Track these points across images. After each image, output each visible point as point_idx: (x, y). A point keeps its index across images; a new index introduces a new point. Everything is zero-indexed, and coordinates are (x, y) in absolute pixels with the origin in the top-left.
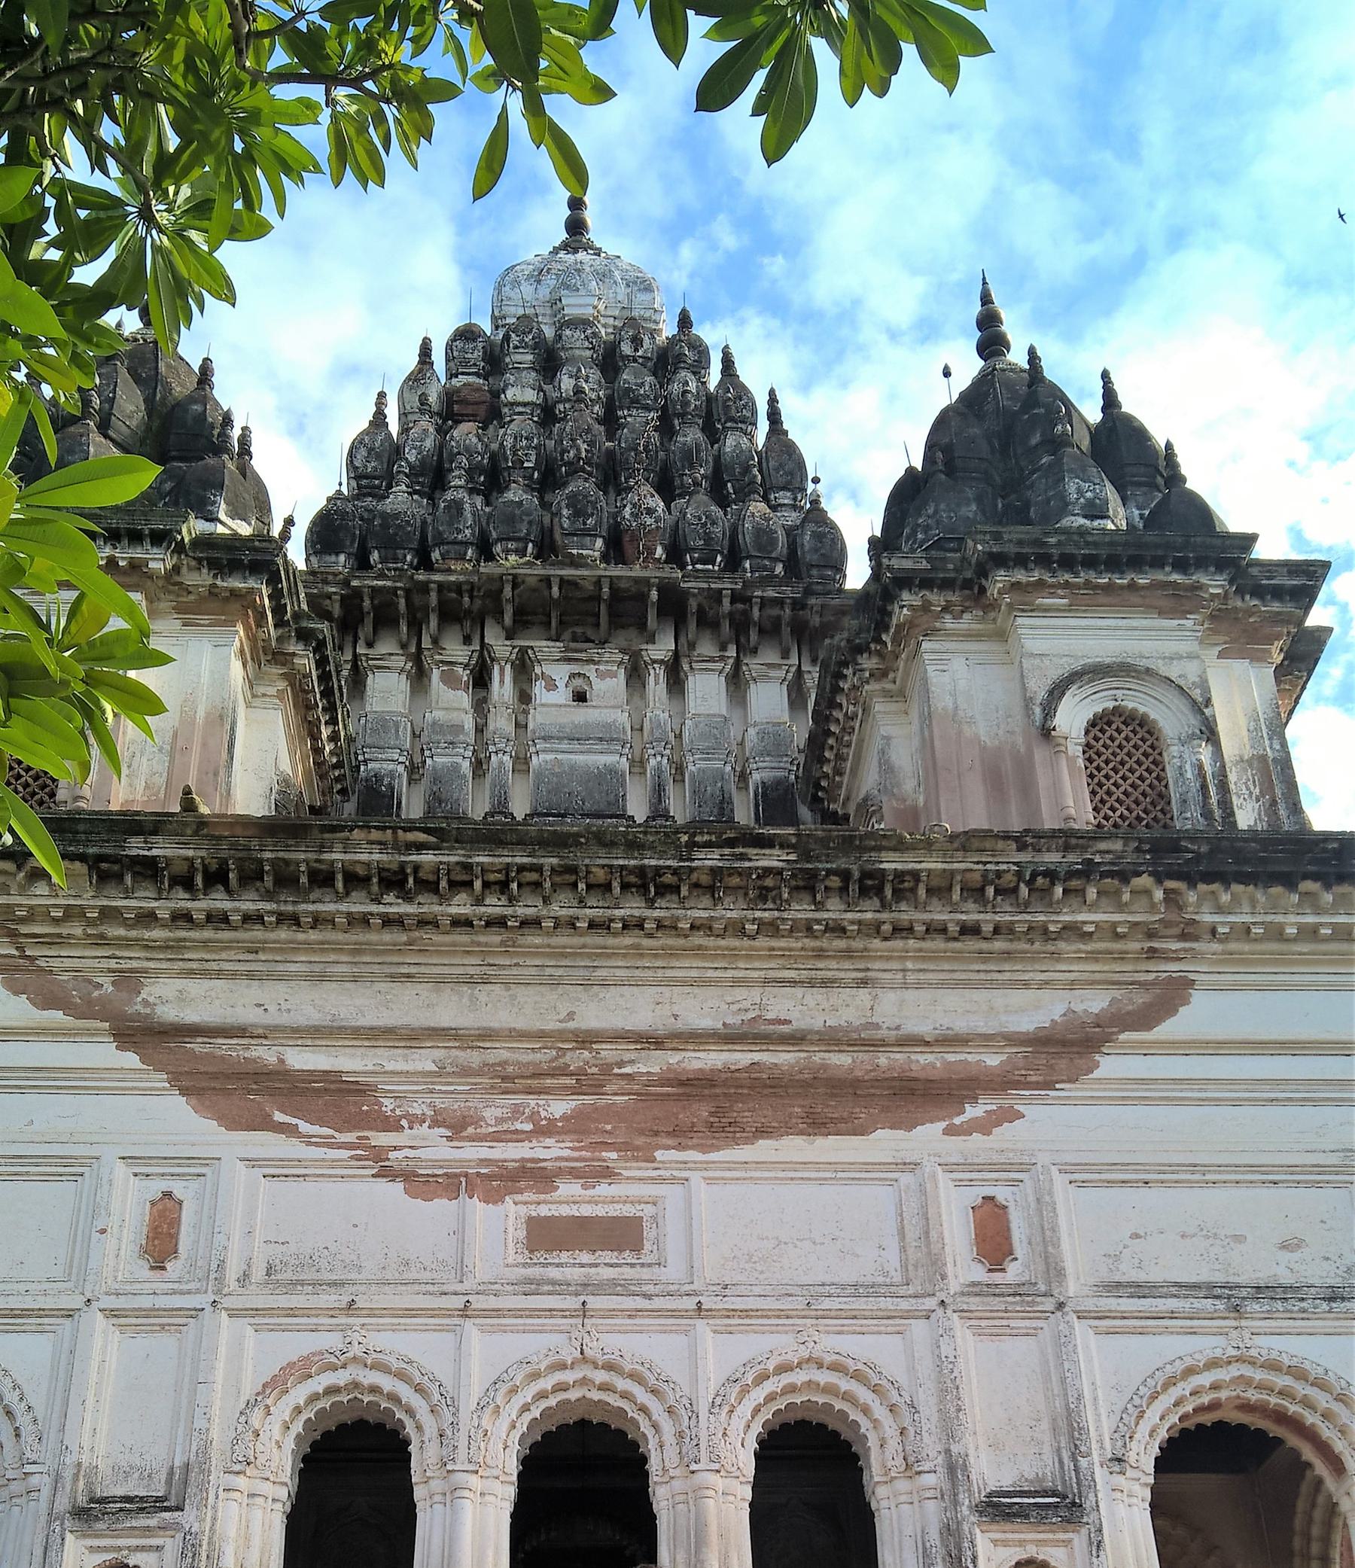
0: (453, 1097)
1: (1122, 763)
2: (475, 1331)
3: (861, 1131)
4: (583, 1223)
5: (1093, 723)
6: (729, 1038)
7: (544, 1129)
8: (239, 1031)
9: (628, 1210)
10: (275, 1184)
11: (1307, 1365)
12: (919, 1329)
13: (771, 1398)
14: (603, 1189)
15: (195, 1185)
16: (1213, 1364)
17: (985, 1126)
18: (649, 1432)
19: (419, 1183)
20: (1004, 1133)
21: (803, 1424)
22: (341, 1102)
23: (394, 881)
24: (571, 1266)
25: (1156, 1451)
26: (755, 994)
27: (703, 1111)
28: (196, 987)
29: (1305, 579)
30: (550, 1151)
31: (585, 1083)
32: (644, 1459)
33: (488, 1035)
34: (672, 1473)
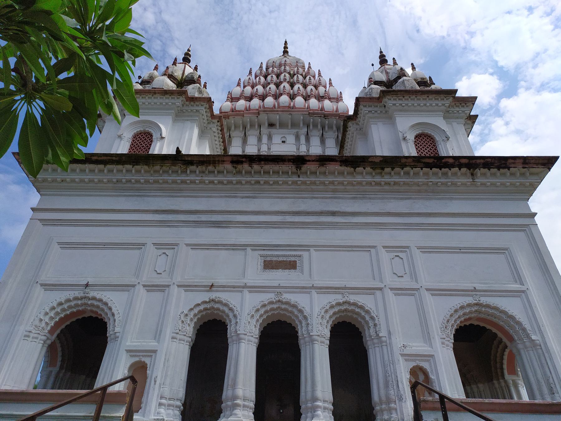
1: (425, 146)
2: (247, 292)
4: (280, 262)
5: (416, 137)
9: (293, 259)
10: (194, 251)
11: (498, 306)
12: (378, 293)
13: (334, 313)
15: (172, 251)
16: (469, 305)
18: (298, 323)
21: (344, 322)
25: (454, 332)
29: (472, 100)
32: (297, 332)
34: (305, 336)
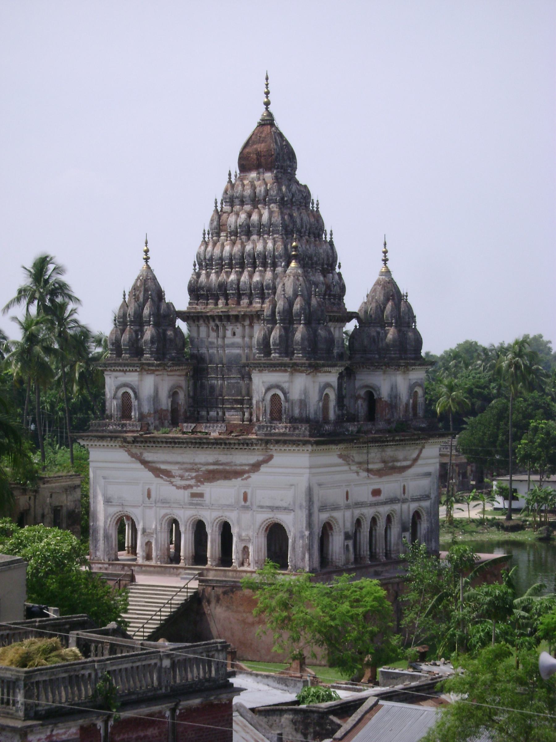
0: (180, 472)
3: (230, 479)
6: (214, 464)
7: (192, 478)
8: (154, 462)
14: (199, 488)
17: (246, 479)
19: (178, 488)
20: (249, 480)
22: (168, 474)
23: (166, 442)
24: (196, 500)
26: (216, 456)
27: (211, 475)
28: (149, 454)
30: (192, 482)
31: (197, 470)
33: (183, 463)
